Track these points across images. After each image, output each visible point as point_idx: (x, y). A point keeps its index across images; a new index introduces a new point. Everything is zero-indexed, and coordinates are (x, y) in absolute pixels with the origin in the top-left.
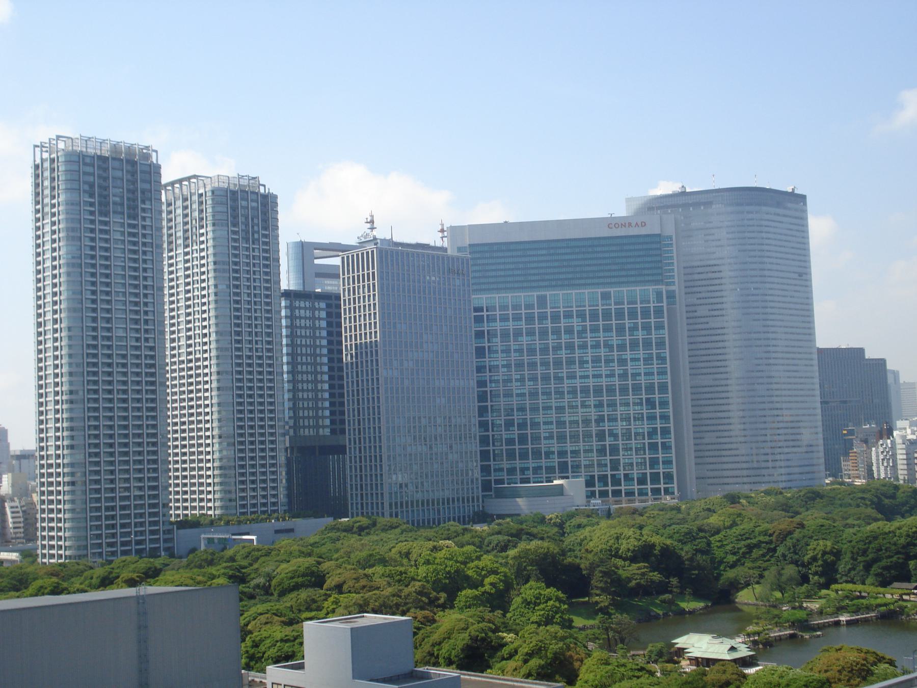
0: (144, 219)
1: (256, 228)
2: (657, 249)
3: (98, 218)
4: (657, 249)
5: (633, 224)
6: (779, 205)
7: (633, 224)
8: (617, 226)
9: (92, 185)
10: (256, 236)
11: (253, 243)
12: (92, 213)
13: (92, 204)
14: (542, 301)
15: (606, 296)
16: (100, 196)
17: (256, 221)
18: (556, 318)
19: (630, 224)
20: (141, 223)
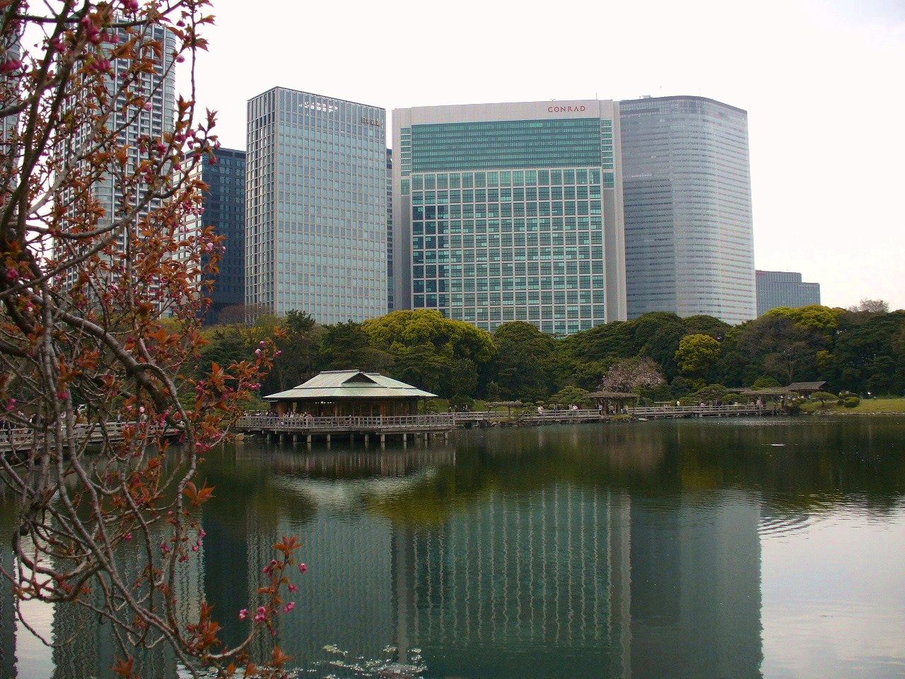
2: (596, 139)
4: (596, 139)
5: (573, 108)
8: (557, 109)
14: (480, 178)
15: (543, 177)
18: (493, 196)
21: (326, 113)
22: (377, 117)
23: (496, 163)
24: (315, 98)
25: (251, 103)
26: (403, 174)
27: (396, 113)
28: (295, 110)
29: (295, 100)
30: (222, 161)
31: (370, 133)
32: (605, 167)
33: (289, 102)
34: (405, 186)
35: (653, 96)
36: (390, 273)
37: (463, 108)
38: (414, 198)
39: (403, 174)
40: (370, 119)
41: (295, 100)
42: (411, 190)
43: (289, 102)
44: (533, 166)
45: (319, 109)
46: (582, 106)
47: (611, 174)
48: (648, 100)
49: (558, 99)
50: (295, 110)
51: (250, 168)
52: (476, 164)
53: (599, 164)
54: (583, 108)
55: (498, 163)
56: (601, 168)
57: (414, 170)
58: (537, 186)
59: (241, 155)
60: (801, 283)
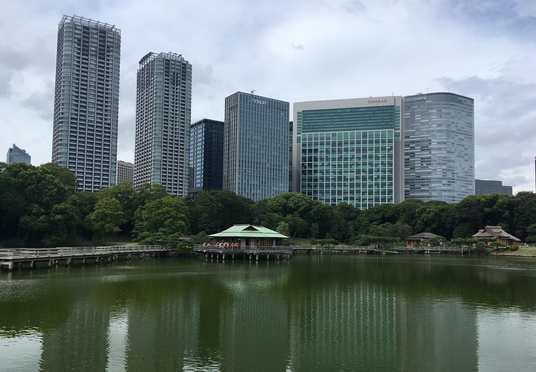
0: (108, 60)
1: (179, 79)
3: (81, 56)
5: (381, 101)
6: (460, 102)
7: (381, 101)
8: (373, 102)
9: (79, 40)
10: (179, 83)
11: (177, 86)
12: (79, 53)
13: (79, 49)
16: (83, 46)
17: (179, 75)
18: (340, 144)
19: (379, 101)
20: (106, 62)
21: (261, 105)
22: (285, 107)
23: (342, 129)
24: (257, 97)
25: (227, 99)
26: (298, 134)
27: (295, 104)
28: (247, 103)
29: (247, 97)
30: (214, 127)
31: (282, 114)
32: (396, 129)
33: (244, 99)
34: (299, 139)
35: (423, 93)
36: (291, 179)
37: (327, 102)
38: (303, 145)
39: (298, 134)
40: (283, 107)
41: (247, 97)
42: (301, 141)
43: (244, 99)
44: (360, 129)
45: (258, 102)
46: (385, 100)
47: (399, 133)
48: (421, 95)
49: (374, 96)
50: (247, 103)
51: (226, 130)
52: (332, 129)
53: (393, 128)
54: (386, 101)
55: (343, 129)
56: (393, 130)
57: (303, 132)
58: (362, 139)
59: (222, 124)
60: (501, 186)
